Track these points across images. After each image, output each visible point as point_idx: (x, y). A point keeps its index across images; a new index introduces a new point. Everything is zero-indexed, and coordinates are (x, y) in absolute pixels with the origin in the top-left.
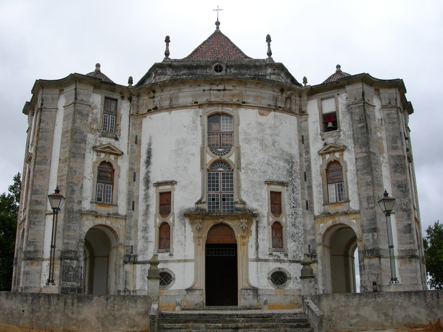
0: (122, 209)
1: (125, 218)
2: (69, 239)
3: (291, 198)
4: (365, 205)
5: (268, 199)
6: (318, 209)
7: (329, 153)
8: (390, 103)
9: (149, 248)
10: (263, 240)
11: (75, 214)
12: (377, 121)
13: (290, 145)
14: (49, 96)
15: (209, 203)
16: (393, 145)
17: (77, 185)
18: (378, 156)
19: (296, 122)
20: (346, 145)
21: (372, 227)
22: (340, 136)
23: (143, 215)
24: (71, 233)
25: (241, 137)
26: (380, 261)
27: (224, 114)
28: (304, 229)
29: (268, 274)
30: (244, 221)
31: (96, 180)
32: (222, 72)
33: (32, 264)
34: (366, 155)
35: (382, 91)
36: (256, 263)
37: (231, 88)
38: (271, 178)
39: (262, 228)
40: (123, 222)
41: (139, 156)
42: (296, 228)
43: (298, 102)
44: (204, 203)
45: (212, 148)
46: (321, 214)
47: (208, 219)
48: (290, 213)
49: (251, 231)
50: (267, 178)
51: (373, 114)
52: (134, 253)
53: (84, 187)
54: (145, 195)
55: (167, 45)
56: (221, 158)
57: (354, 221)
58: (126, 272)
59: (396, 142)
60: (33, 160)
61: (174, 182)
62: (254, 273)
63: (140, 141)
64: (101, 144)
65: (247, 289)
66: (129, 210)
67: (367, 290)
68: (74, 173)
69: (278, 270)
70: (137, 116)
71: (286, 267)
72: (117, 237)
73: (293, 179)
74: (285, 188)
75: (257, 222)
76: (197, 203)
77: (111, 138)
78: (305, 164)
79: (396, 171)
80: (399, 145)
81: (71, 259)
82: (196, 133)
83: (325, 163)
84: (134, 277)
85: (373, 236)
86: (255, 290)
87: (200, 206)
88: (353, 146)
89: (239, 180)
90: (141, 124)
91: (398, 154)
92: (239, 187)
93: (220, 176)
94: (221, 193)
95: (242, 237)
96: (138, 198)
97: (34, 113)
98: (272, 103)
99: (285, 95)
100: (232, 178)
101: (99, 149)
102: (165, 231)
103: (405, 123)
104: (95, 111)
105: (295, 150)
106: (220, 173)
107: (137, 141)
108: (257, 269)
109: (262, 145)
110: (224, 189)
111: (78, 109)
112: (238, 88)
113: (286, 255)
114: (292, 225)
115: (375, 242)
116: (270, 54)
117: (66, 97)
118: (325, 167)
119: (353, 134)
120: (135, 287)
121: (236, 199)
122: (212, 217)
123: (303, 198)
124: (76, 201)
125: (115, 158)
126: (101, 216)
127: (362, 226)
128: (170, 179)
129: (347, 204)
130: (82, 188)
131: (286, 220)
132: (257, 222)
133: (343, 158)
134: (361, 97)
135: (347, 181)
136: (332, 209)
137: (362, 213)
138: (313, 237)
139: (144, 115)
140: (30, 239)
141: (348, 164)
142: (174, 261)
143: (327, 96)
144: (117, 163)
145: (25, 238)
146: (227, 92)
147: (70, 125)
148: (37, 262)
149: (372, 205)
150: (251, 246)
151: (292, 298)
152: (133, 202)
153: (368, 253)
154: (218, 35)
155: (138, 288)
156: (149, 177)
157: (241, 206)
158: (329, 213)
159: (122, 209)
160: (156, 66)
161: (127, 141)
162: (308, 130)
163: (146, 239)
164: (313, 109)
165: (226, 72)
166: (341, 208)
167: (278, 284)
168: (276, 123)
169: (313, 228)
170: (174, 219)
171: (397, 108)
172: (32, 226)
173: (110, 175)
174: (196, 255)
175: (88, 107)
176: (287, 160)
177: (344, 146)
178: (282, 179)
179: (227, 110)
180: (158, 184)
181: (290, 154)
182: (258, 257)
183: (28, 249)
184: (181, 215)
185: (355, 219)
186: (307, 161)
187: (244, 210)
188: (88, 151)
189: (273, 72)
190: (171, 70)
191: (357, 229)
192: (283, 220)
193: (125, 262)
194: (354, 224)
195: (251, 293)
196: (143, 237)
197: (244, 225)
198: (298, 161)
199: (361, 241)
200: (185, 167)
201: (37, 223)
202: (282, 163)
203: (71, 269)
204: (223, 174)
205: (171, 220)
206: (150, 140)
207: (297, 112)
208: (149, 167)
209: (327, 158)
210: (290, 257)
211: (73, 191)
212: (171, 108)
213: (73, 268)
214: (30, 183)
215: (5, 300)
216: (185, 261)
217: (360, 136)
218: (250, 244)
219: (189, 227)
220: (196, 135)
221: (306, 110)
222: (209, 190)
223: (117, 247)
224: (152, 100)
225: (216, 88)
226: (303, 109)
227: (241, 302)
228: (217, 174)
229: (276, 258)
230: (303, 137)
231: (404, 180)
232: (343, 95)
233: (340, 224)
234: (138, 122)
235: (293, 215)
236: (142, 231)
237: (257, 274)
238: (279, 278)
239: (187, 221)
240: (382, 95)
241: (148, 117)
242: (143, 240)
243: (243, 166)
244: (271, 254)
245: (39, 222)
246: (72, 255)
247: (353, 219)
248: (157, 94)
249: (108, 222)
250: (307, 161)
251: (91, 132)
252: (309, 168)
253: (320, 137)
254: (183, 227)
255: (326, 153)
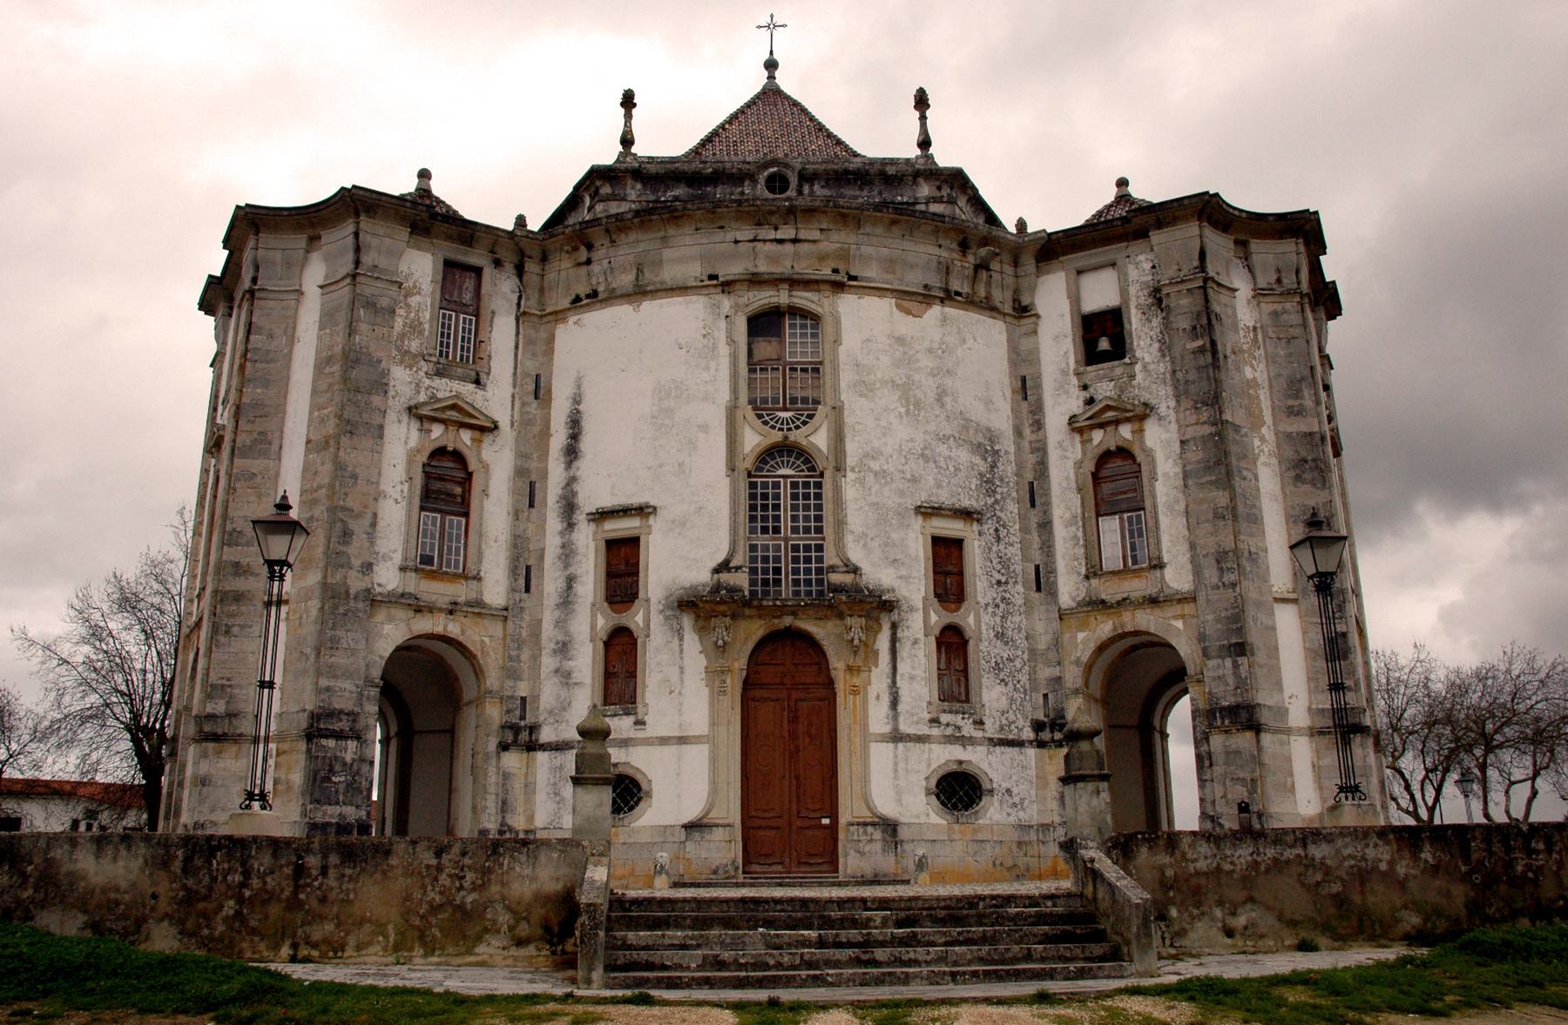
0: (495, 590)
1: (504, 614)
2: (335, 677)
3: (993, 555)
4: (1211, 575)
5: (926, 559)
6: (1069, 588)
7: (1101, 426)
8: (1279, 281)
9: (574, 704)
10: (912, 678)
11: (352, 603)
12: (1242, 333)
13: (988, 403)
14: (277, 256)
15: (753, 571)
16: (1291, 402)
17: (359, 516)
18: (1246, 435)
19: (1004, 337)
20: (1153, 402)
21: (1234, 641)
22: (1132, 377)
23: (558, 606)
24: (340, 659)
25: (846, 377)
26: (1258, 741)
27: (794, 311)
28: (1032, 649)
29: (927, 778)
30: (855, 622)
31: (417, 502)
32: (788, 193)
33: (219, 753)
34: (1213, 429)
35: (1256, 246)
36: (891, 745)
37: (816, 235)
38: (934, 499)
39: (909, 644)
40: (497, 629)
41: (545, 434)
42: (1006, 643)
43: (1009, 280)
44: (738, 568)
45: (761, 408)
46: (1078, 604)
47: (751, 617)
48: (989, 599)
49: (876, 653)
50: (921, 497)
51: (1230, 311)
52: (530, 719)
53: (381, 524)
54: (563, 546)
55: (628, 117)
56: (786, 438)
57: (1179, 624)
58: (506, 776)
59: (1298, 395)
60: (226, 446)
61: (648, 507)
62: (886, 777)
63: (549, 391)
64: (433, 396)
65: (865, 824)
66: (514, 590)
67: (1221, 825)
68: (351, 481)
69: (954, 767)
70: (538, 321)
71: (980, 759)
72: (478, 672)
73: (996, 502)
74: (975, 526)
75: (894, 626)
76: (717, 571)
77: (463, 379)
78: (1031, 459)
79: (1298, 478)
80: (1308, 402)
81: (339, 736)
82: (712, 364)
83: (1089, 455)
84: (530, 789)
85: (1236, 666)
86: (890, 827)
87: (724, 577)
88: (1172, 404)
89: (839, 502)
90: (551, 340)
91: (1305, 429)
92: (840, 524)
93: (785, 492)
94: (786, 539)
95: (850, 669)
96: (542, 557)
97: (231, 308)
98: (935, 281)
99: (971, 259)
100: (818, 496)
101: (425, 411)
102: (621, 651)
103: (1319, 342)
104: (414, 300)
105: (1001, 418)
106: (784, 481)
107: (540, 390)
108: (896, 764)
109: (907, 400)
110: (795, 530)
111: (361, 293)
112: (835, 236)
113: (979, 723)
114: (996, 636)
115: (1242, 684)
116: (925, 143)
117: (328, 259)
118: (1090, 466)
119: (1174, 372)
120: (531, 818)
121: (830, 558)
122: (762, 612)
123: (1025, 558)
124: (356, 563)
125: (473, 440)
126: (431, 609)
127: (1202, 638)
128: (636, 500)
129: (1158, 573)
130: (374, 525)
131: (976, 619)
132: (894, 626)
133: (1142, 441)
134: (1196, 263)
135: (1155, 506)
136: (1109, 590)
137: (1201, 601)
138: (1056, 672)
139: (559, 316)
140: (213, 678)
141: (1160, 456)
142: (648, 742)
143: (1094, 261)
144: (479, 454)
145: (199, 677)
146: (804, 248)
147: (340, 339)
148: (234, 749)
149: (1233, 577)
150: (878, 698)
151: (997, 850)
152: (528, 568)
153: (1223, 719)
154: (771, 95)
155: (539, 822)
156: (574, 494)
157: (847, 579)
158: (1103, 602)
159: (495, 588)
160: (597, 175)
161: (511, 390)
162: (1039, 360)
163: (565, 676)
164: (1054, 298)
165: (800, 192)
166: (1137, 587)
167: (955, 807)
168: (947, 339)
169: (1057, 644)
170: (649, 618)
171: (1302, 295)
172: (222, 639)
173: (458, 490)
174: (713, 724)
175: (395, 288)
176: (979, 445)
177: (1146, 405)
178: (966, 502)
179: (804, 299)
180: (601, 516)
181: (988, 430)
182: (896, 729)
183: (209, 709)
184: (667, 607)
185: (1182, 617)
186: (1038, 450)
187: (857, 589)
188: (391, 416)
189: (937, 194)
190: (639, 186)
191: (1186, 648)
192: (968, 619)
193: (504, 747)
194: (1178, 631)
195: (878, 835)
196: (557, 671)
197: (857, 634)
198: (1012, 449)
199: (1199, 681)
200: (680, 465)
201: (235, 630)
202: (964, 456)
203: (337, 768)
204: (794, 485)
205: (639, 619)
206: (579, 387)
207: (1008, 308)
208: (576, 464)
209: (1095, 442)
210: (991, 729)
211: (346, 535)
212: (640, 292)
213: (345, 764)
214: (218, 512)
215: (91, 859)
216: (682, 740)
217: (1193, 376)
218: (872, 691)
219: (692, 641)
220: (713, 372)
221: (1032, 304)
222: (753, 531)
223: (479, 702)
224: (584, 269)
225: (772, 235)
226: (1025, 301)
227: (851, 862)
228: (776, 485)
229: (949, 731)
230: (1024, 380)
231: (1325, 504)
232: (1141, 258)
233: (1136, 633)
234: (543, 335)
235: (997, 606)
236: (555, 652)
237: (896, 778)
238: (959, 791)
239: (687, 621)
240: (1256, 259)
241: (572, 319)
242: (555, 680)
243: (851, 461)
244: (935, 721)
245: (242, 627)
246: (343, 725)
247: (1176, 617)
248: (598, 254)
249: (453, 628)
250: (1038, 450)
251: (402, 362)
252: (1042, 468)
253: (1074, 381)
254: (676, 641)
255: (1092, 427)
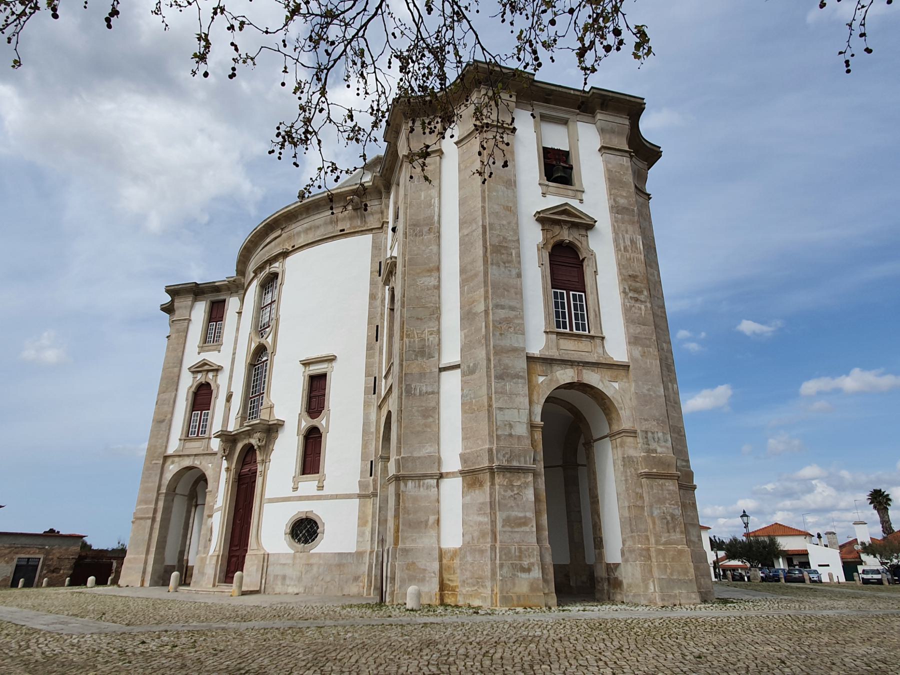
113: (320, 488)
179: (276, 267)
192: (321, 422)
238: (305, 530)
244: (295, 489)
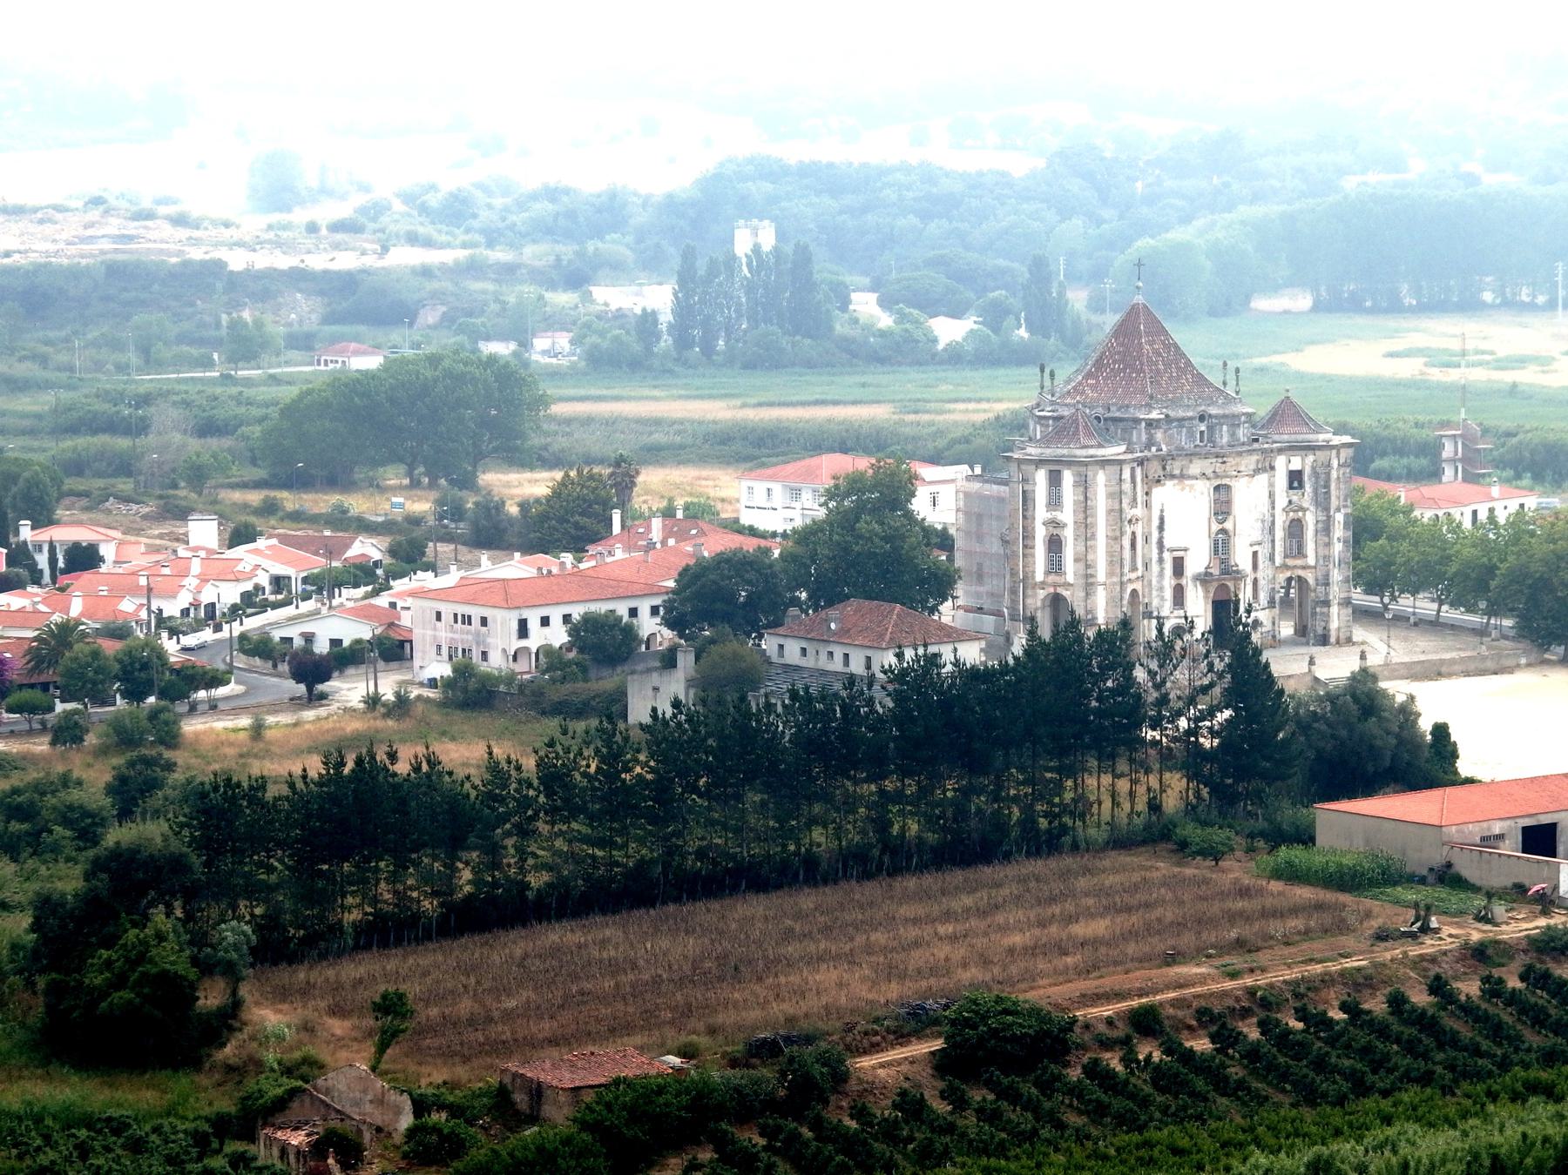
6: (1278, 560)
102: (1179, 592)
128: (1183, 546)
136: (1290, 562)
163: (1162, 599)
170: (1187, 581)
191: (1311, 581)
194: (1310, 577)
